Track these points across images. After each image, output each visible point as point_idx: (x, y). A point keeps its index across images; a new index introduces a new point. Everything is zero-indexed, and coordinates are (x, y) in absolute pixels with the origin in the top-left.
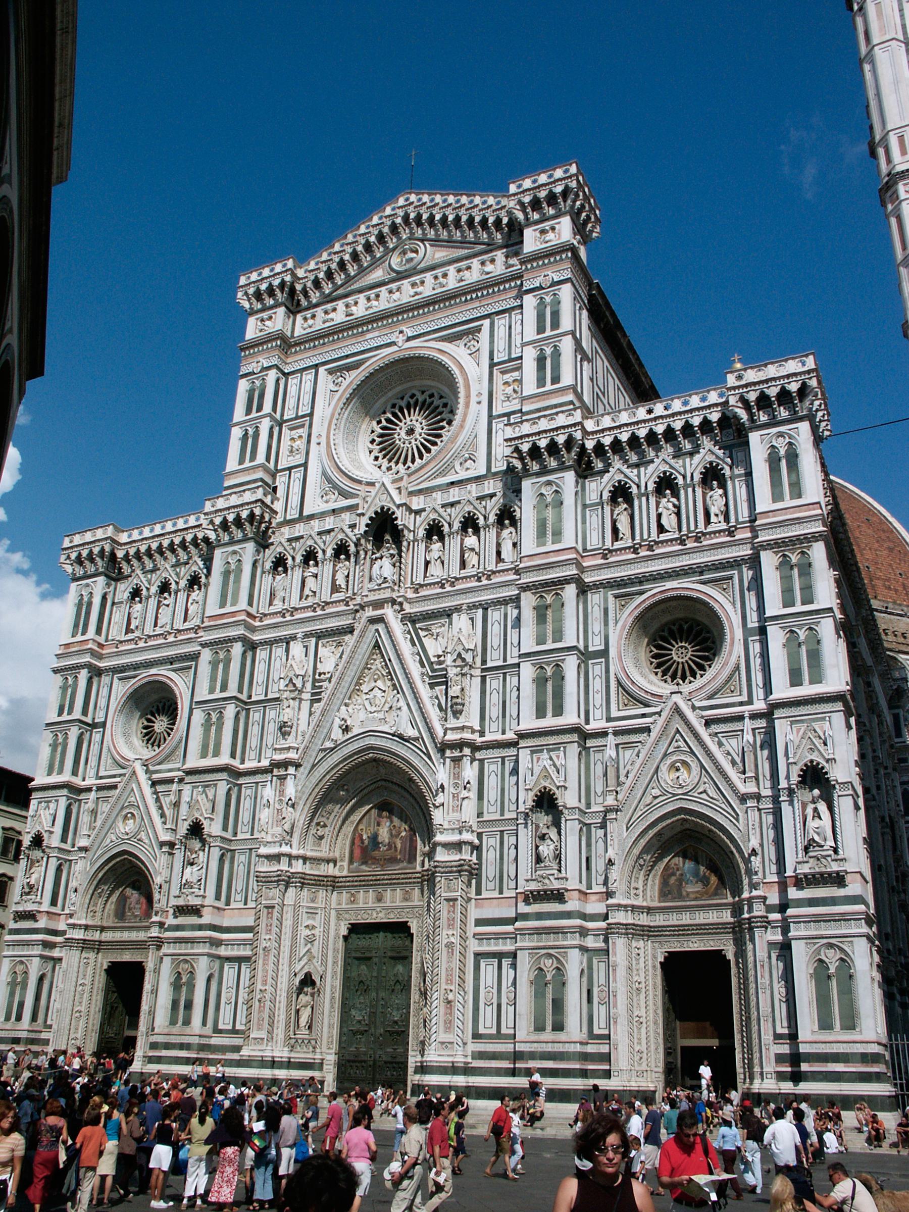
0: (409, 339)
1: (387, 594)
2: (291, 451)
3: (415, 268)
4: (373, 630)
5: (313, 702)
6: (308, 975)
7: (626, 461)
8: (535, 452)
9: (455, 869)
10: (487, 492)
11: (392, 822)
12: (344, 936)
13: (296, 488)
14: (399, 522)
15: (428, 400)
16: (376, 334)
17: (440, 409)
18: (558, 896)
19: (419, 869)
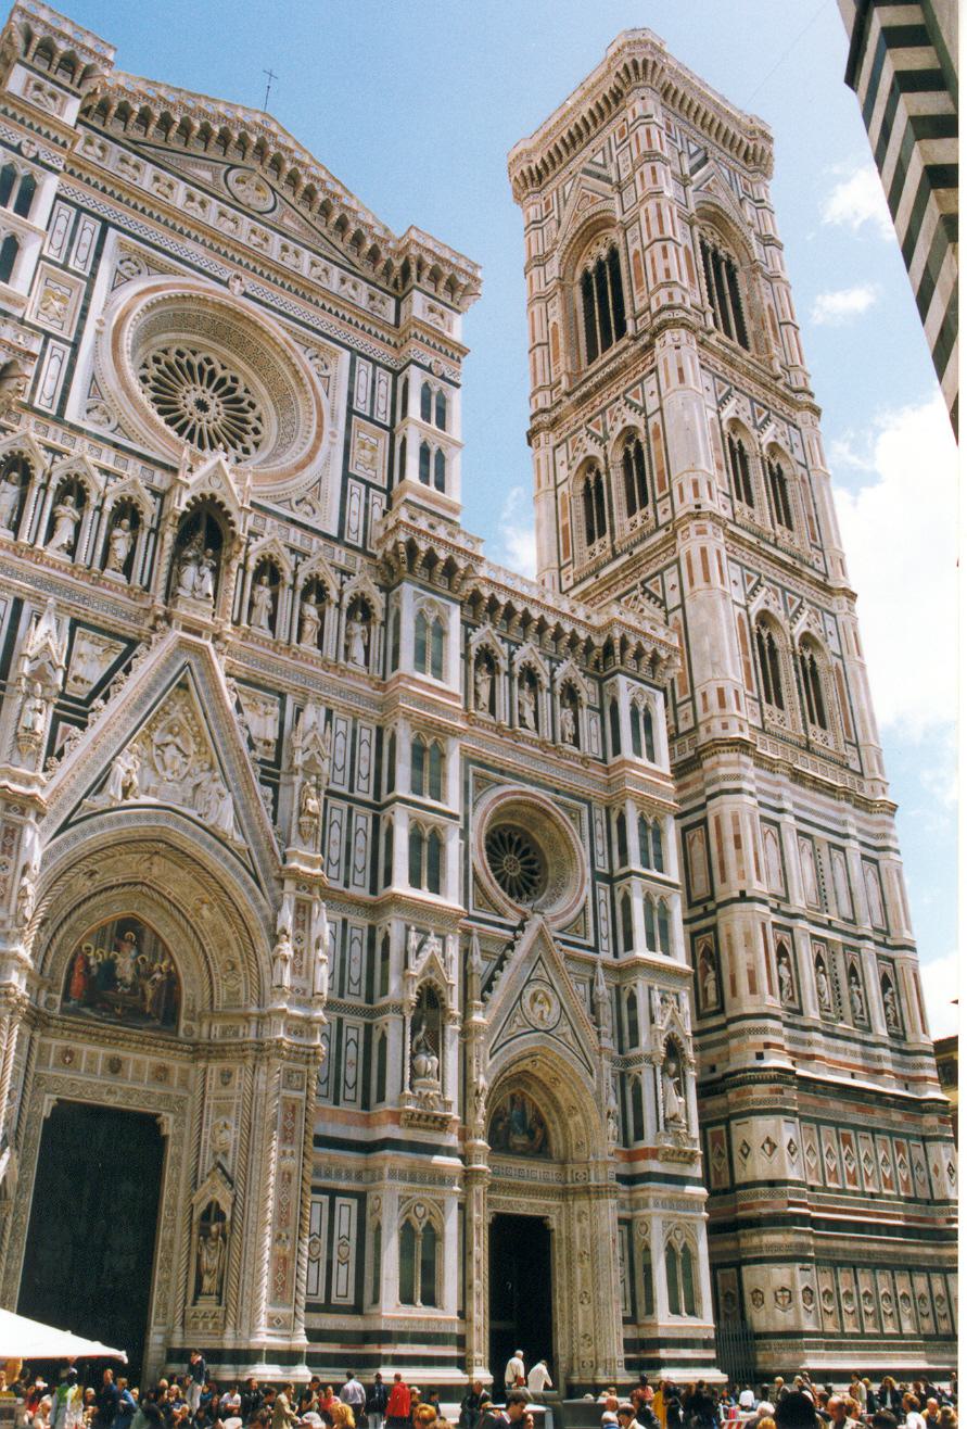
0: (245, 294)
2: (45, 309)
3: (261, 213)
7: (495, 627)
8: (431, 559)
10: (336, 560)
11: (140, 951)
12: (45, 1120)
14: (239, 529)
15: (229, 383)
16: (200, 250)
17: (244, 405)
18: (442, 1124)
19: (181, 1034)
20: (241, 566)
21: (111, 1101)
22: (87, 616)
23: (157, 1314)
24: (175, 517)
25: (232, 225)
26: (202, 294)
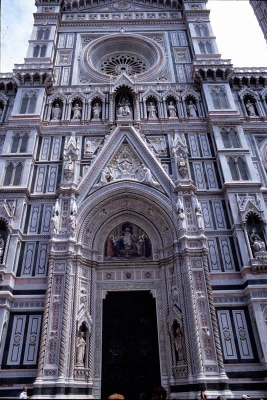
0: (126, 31)
1: (130, 120)
2: (62, 61)
4: (123, 135)
5: (82, 166)
6: (84, 324)
7: (249, 87)
8: (210, 73)
9: (199, 254)
10: (177, 89)
11: (132, 234)
12: (103, 300)
13: (66, 74)
15: (131, 60)
17: (138, 63)
19: (154, 259)
20: (140, 103)
21: (129, 290)
22: (87, 133)
23: (163, 371)
24: (111, 95)
25: (117, 17)
26: (110, 37)
